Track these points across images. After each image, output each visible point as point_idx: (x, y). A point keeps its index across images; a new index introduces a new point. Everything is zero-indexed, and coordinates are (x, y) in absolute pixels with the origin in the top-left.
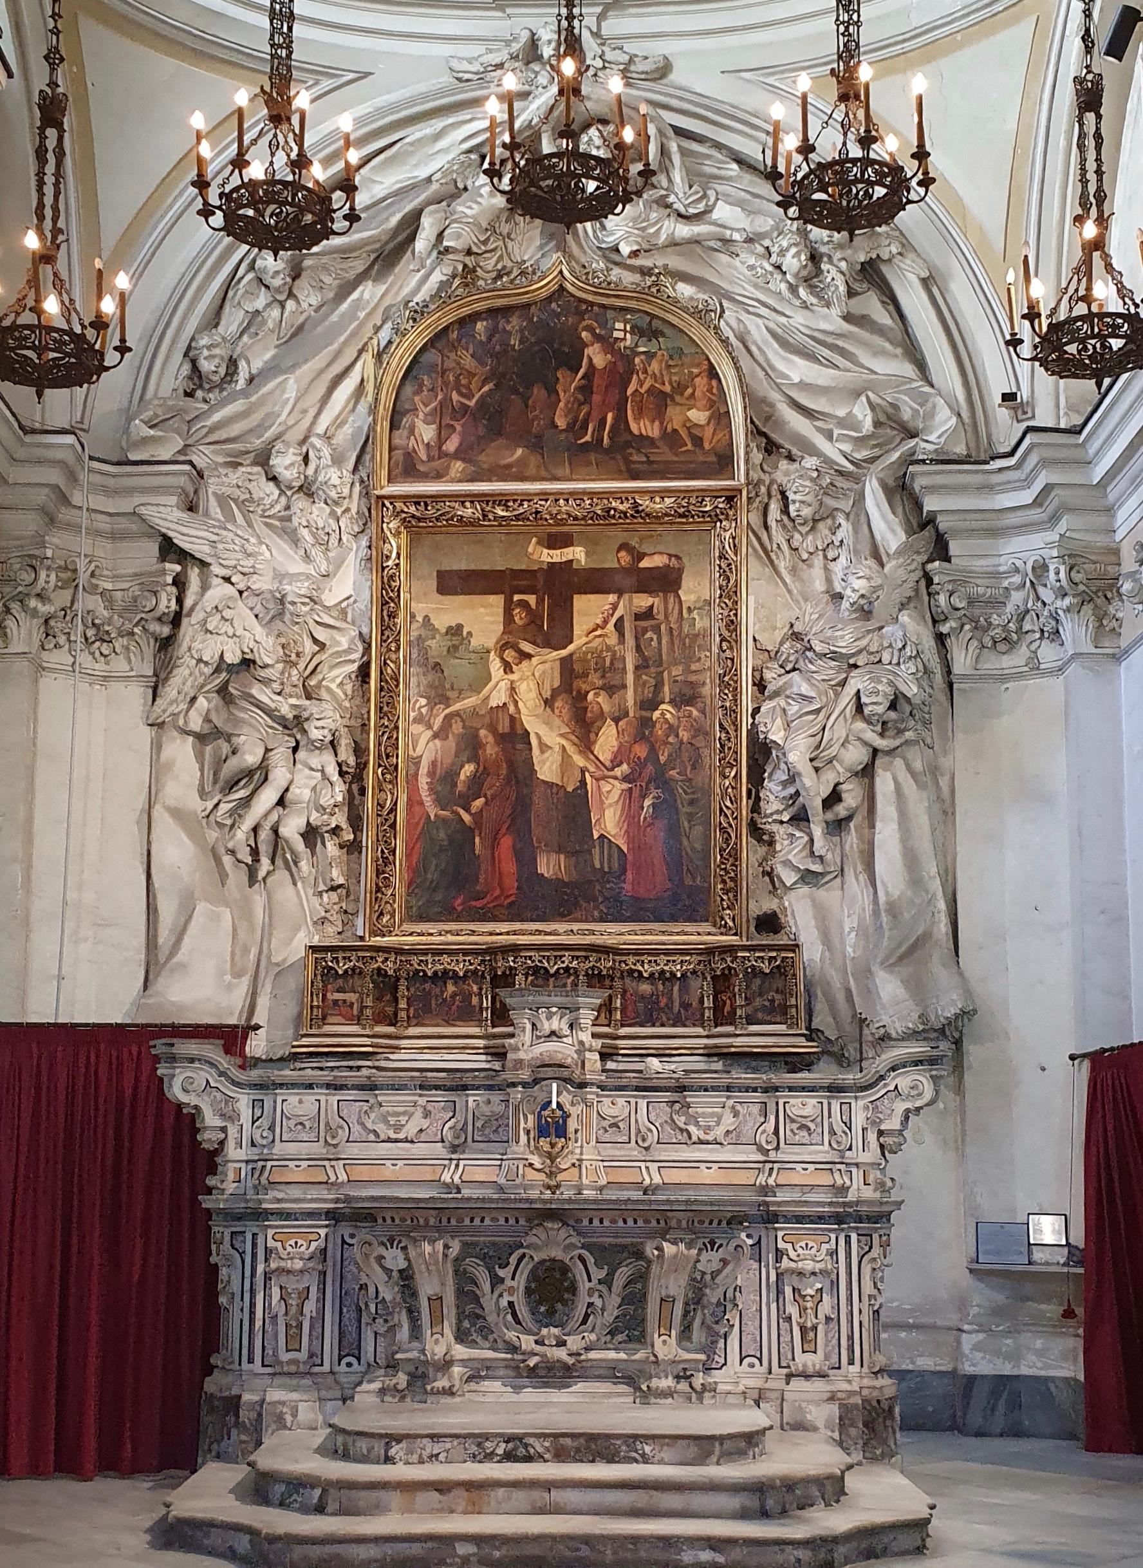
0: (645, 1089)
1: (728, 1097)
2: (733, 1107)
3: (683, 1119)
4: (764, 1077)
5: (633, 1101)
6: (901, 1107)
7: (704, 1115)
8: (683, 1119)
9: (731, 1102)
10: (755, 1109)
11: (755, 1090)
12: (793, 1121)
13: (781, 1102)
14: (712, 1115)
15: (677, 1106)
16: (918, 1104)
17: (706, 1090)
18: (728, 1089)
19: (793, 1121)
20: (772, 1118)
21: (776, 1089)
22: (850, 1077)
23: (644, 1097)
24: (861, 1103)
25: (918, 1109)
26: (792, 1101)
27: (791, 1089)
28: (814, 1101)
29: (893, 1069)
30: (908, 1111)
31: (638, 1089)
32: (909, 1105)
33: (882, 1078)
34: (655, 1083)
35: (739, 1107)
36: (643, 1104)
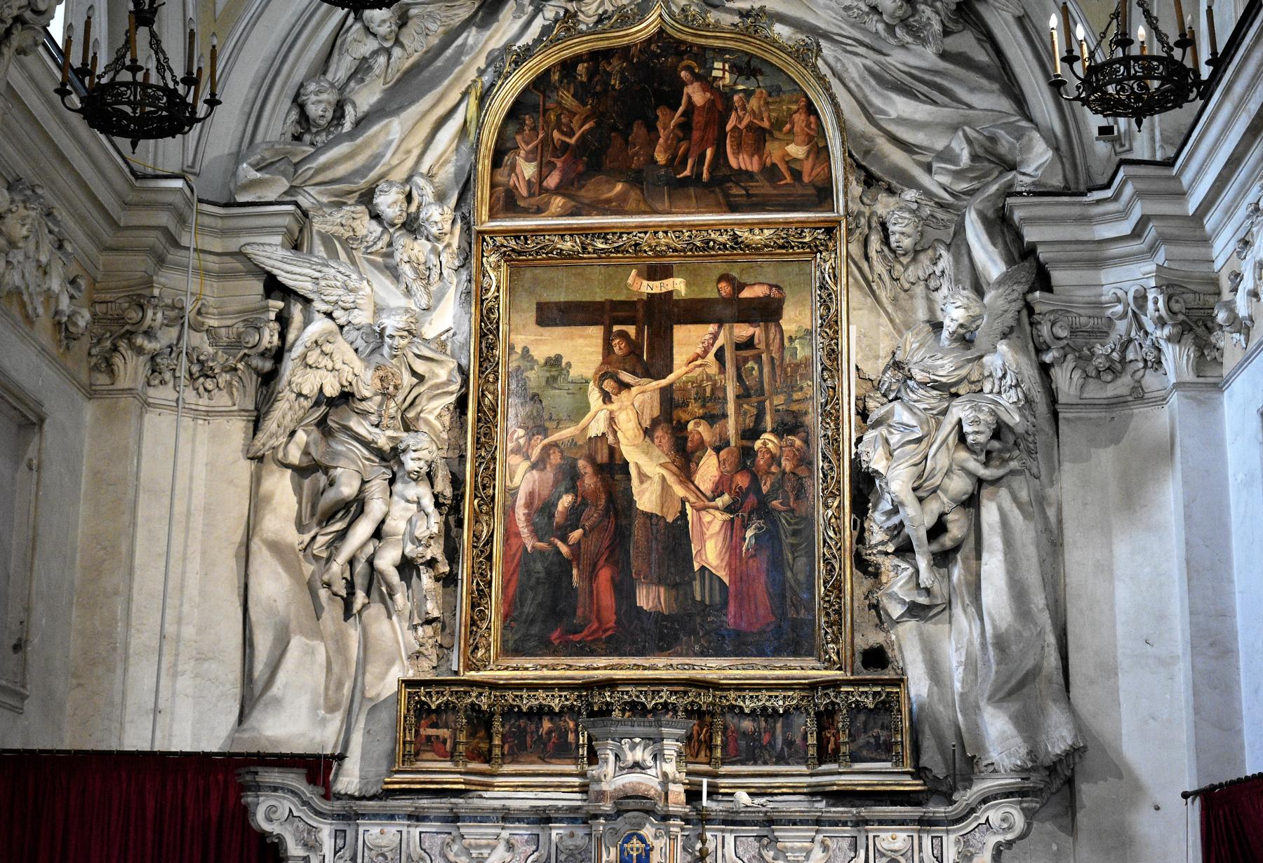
0: (734, 823)
1: (817, 832)
2: (823, 842)
3: (771, 853)
4: (854, 810)
5: (719, 835)
6: (992, 840)
7: (793, 850)
8: (771, 853)
9: (820, 837)
10: (845, 844)
11: (845, 824)
12: (883, 855)
13: (871, 835)
14: (801, 850)
15: (765, 841)
16: (1010, 837)
17: (795, 824)
18: (818, 822)
19: (883, 855)
20: (862, 853)
21: (867, 822)
22: (940, 811)
23: (732, 831)
24: (953, 837)
25: (1010, 844)
26: (882, 835)
27: (881, 822)
28: (904, 835)
29: (985, 801)
30: (998, 845)
31: (725, 822)
32: (1000, 838)
33: (973, 810)
34: (742, 817)
35: (828, 842)
36: (730, 839)
